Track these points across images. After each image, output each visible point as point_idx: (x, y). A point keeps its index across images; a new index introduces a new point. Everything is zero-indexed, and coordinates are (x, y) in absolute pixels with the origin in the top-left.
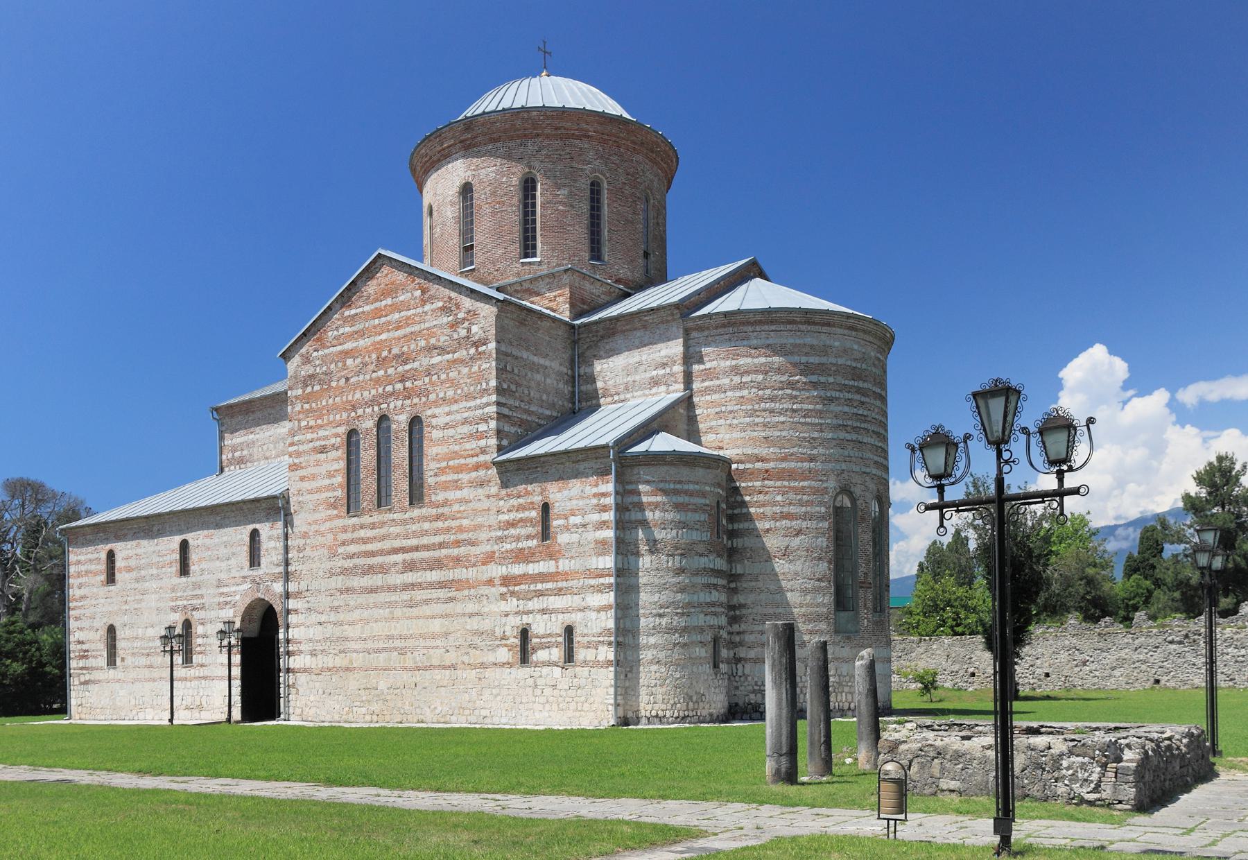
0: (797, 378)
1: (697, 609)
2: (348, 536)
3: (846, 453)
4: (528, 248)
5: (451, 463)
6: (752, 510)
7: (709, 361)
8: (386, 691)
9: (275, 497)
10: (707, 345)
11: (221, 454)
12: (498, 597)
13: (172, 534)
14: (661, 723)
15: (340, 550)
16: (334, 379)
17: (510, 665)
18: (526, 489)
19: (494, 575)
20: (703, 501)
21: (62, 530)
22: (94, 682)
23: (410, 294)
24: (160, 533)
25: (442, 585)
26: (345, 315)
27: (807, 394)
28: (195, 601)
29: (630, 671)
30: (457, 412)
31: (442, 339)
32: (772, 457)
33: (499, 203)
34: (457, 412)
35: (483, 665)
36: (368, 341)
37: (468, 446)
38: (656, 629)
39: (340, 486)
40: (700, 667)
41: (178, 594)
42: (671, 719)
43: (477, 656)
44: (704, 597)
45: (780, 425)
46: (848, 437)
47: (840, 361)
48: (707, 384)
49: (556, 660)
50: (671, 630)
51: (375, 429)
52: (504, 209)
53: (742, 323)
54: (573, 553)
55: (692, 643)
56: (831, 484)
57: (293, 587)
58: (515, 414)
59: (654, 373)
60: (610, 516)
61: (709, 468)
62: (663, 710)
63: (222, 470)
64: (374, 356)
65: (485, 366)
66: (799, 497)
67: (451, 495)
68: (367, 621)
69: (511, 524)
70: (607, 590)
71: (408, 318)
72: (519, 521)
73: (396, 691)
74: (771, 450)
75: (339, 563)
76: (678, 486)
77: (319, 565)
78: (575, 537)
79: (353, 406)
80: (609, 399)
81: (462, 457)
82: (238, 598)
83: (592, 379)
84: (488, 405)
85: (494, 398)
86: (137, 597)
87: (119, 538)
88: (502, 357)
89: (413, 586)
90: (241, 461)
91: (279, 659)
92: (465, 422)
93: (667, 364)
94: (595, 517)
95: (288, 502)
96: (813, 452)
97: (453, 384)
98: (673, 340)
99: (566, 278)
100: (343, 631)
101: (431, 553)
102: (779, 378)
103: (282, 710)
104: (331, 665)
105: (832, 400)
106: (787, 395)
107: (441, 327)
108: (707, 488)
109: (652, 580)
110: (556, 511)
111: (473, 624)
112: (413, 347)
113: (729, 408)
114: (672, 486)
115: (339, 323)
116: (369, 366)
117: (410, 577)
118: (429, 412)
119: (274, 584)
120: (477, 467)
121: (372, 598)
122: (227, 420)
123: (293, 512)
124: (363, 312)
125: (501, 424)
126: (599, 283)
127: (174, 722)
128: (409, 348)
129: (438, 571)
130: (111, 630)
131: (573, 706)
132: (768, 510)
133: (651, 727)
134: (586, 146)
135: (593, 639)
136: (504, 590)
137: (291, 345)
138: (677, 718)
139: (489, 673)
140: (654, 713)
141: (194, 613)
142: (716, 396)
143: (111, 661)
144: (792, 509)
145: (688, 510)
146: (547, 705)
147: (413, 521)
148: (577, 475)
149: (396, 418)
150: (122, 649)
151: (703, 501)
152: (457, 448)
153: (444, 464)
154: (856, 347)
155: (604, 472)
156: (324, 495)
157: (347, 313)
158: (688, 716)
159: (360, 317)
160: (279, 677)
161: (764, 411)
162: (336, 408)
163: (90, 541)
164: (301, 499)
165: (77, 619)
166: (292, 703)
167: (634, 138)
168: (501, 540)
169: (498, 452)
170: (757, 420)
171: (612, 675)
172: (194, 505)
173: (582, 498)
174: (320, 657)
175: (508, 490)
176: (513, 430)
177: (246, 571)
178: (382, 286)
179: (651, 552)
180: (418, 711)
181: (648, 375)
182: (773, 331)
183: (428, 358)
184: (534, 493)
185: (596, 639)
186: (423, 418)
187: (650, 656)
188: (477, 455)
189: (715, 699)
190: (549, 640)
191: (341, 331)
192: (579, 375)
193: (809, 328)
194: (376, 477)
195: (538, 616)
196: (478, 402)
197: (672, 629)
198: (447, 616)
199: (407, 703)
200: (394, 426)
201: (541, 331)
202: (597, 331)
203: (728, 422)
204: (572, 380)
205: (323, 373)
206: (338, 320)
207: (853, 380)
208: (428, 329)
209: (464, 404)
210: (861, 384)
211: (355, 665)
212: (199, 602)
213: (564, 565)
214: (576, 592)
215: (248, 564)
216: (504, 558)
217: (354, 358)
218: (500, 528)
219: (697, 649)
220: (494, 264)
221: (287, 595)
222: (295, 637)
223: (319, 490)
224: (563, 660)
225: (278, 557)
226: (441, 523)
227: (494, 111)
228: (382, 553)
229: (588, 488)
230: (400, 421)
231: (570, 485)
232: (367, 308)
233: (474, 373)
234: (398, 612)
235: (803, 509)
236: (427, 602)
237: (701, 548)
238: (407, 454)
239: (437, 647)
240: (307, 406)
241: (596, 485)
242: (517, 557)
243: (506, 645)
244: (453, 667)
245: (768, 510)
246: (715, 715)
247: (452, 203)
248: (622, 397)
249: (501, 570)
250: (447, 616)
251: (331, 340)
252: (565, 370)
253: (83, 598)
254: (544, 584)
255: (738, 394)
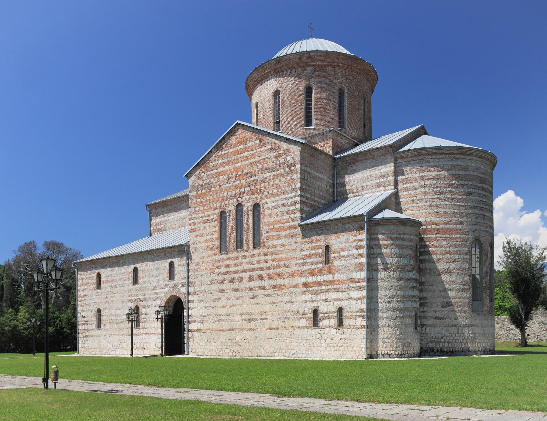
0: (454, 182)
1: (408, 299)
2: (221, 264)
3: (478, 221)
4: (308, 121)
5: (275, 226)
6: (430, 249)
7: (408, 174)
8: (240, 341)
9: (183, 245)
10: (407, 166)
11: (150, 227)
12: (301, 293)
13: (129, 264)
14: (390, 357)
15: (216, 271)
16: (213, 186)
17: (308, 328)
18: (316, 238)
19: (299, 282)
21: (75, 263)
22: (90, 336)
23: (253, 143)
24: (123, 264)
25: (270, 287)
26: (219, 154)
27: (459, 190)
28: (141, 297)
29: (373, 331)
30: (279, 200)
31: (271, 164)
32: (441, 222)
33: (293, 99)
34: (279, 200)
35: (293, 328)
36: (231, 167)
37: (285, 217)
38: (387, 309)
39: (216, 239)
40: (409, 329)
41: (132, 294)
42: (394, 356)
43: (289, 323)
44: (411, 293)
45: (445, 206)
46: (479, 212)
48: (406, 186)
49: (333, 325)
50: (395, 310)
51: (235, 211)
52: (296, 102)
53: (426, 154)
54: (343, 270)
55: (405, 316)
56: (471, 236)
57: (191, 289)
58: (308, 202)
59: (378, 181)
60: (364, 251)
61: (413, 227)
62: (391, 351)
63: (151, 235)
64: (234, 174)
65: (294, 177)
66: (454, 243)
67: (276, 242)
68: (230, 306)
69: (309, 256)
70: (362, 289)
71: (253, 154)
72: (312, 255)
73: (245, 341)
74: (440, 219)
75: (215, 277)
76: (399, 236)
77: (205, 279)
78: (344, 262)
79: (223, 199)
80: (353, 195)
81: (281, 223)
82: (163, 295)
83: (344, 185)
84: (296, 196)
85: (299, 193)
86: (112, 295)
87: (103, 267)
88: (302, 172)
89: (255, 288)
90: (160, 230)
91: (184, 325)
92: (283, 205)
93: (384, 176)
94: (355, 252)
95: (189, 248)
96: (461, 220)
97: (277, 187)
98: (388, 164)
99: (330, 135)
100: (217, 311)
101: (265, 272)
102: (444, 182)
103: (186, 349)
104: (211, 328)
105: (471, 193)
106: (449, 191)
107: (270, 158)
108: (412, 237)
109: (385, 284)
110: (333, 249)
111: (288, 307)
112: (255, 169)
113: (418, 198)
114: (395, 236)
115: (215, 158)
116: (231, 179)
117: (253, 284)
118: (264, 201)
119: (182, 288)
120: (289, 228)
121: (233, 295)
122: (153, 211)
123: (191, 252)
124: (228, 153)
125: (302, 206)
126: (345, 138)
127: (133, 356)
128: (253, 169)
129: (268, 281)
130: (99, 311)
131: (342, 348)
132: (439, 249)
133: (385, 359)
134: (337, 71)
135: (354, 314)
136: (305, 289)
137: (191, 170)
138: (398, 355)
139: (296, 332)
140: (386, 352)
141: (140, 302)
142: (411, 192)
143: (99, 326)
144: (451, 249)
145: (404, 248)
146: (328, 348)
147: (255, 255)
148: (345, 230)
149: (246, 204)
150: (104, 320)
152: (279, 219)
153: (271, 227)
155: (360, 229)
156: (208, 244)
157: (220, 153)
158: (403, 354)
159: (227, 155)
160: (184, 333)
161: (437, 199)
162: (214, 201)
163: (88, 268)
164: (195, 246)
165: (82, 306)
166: (190, 347)
167: (360, 67)
168: (302, 264)
169: (301, 220)
170: (433, 204)
171: (364, 333)
172: (141, 250)
173: (348, 242)
174: (205, 324)
175: (307, 239)
176: (307, 209)
177: (167, 282)
178: (239, 139)
179: (385, 270)
180: (257, 351)
181: (375, 182)
182: (442, 158)
183: (263, 174)
184: (321, 240)
185: (355, 314)
186: (261, 204)
187: (384, 323)
188: (289, 222)
190: (329, 315)
191: (217, 162)
192: (337, 183)
193: (460, 157)
194: (235, 234)
195: (323, 303)
196: (290, 195)
197: (395, 309)
198: (273, 303)
199: (251, 346)
200: (244, 209)
201: (320, 161)
202: (347, 161)
203: (417, 205)
204: (333, 186)
205: (207, 184)
206: (215, 157)
208: (263, 159)
209: (282, 196)
211: (224, 328)
212: (143, 297)
213: (337, 276)
214: (344, 289)
215: (168, 278)
216: (304, 274)
217: (224, 175)
218: (302, 259)
219: (408, 320)
220: (291, 130)
221: (188, 294)
222: (192, 314)
223: (205, 241)
224: (337, 325)
225: (184, 274)
226: (270, 256)
227: (292, 54)
228: (238, 272)
229: (351, 237)
230: (248, 206)
231: (341, 236)
232: (230, 151)
233: (288, 181)
234: (247, 301)
235: (457, 249)
236: (262, 296)
237: (409, 268)
238: (252, 223)
239: (268, 319)
240: (199, 200)
241: (356, 236)
242: (311, 273)
243: (305, 318)
244: (277, 329)
245: (439, 249)
246: (416, 354)
247: (269, 101)
248: (360, 193)
249: (304, 280)
250: (273, 303)
251: (211, 167)
252: (330, 181)
253: (85, 296)
254: (326, 287)
255: (423, 190)
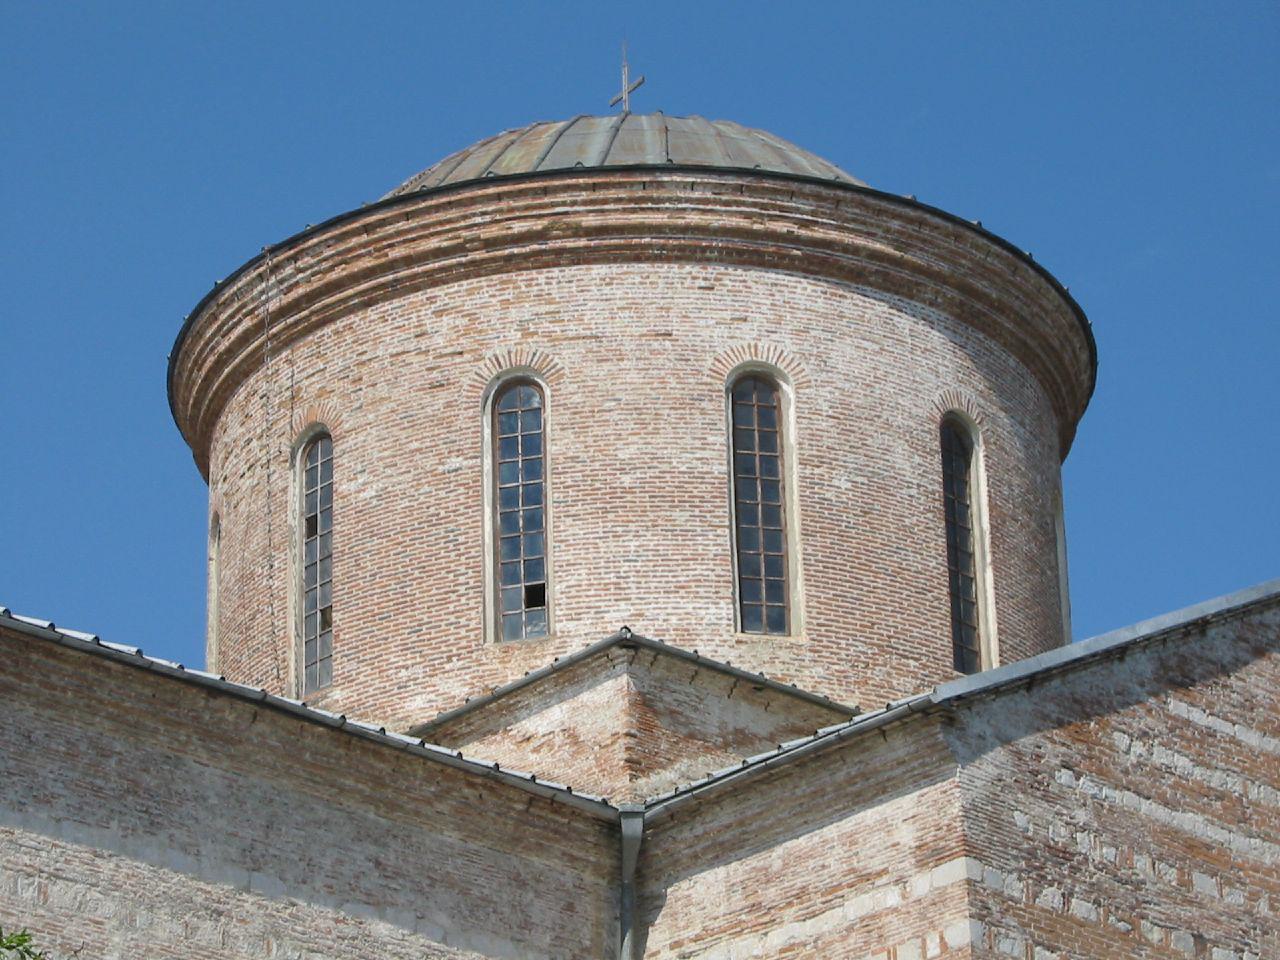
232: (1252, 738)
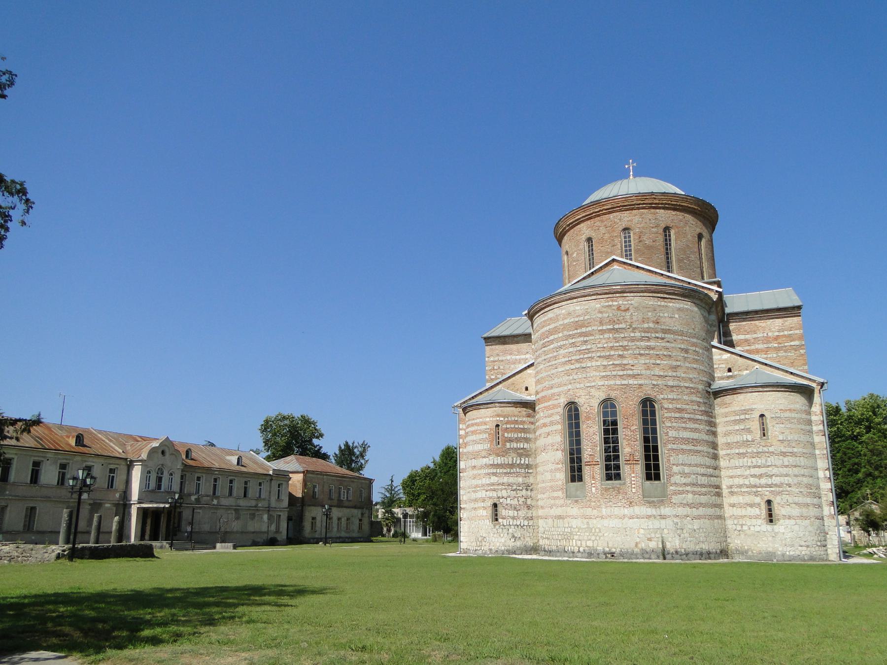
20: (485, 427)
46: (573, 367)
47: (566, 321)
105: (560, 347)
108: (488, 419)
151: (485, 427)
154: (578, 308)
189: (493, 540)
207: (577, 329)
210: (584, 330)
237: (484, 453)
